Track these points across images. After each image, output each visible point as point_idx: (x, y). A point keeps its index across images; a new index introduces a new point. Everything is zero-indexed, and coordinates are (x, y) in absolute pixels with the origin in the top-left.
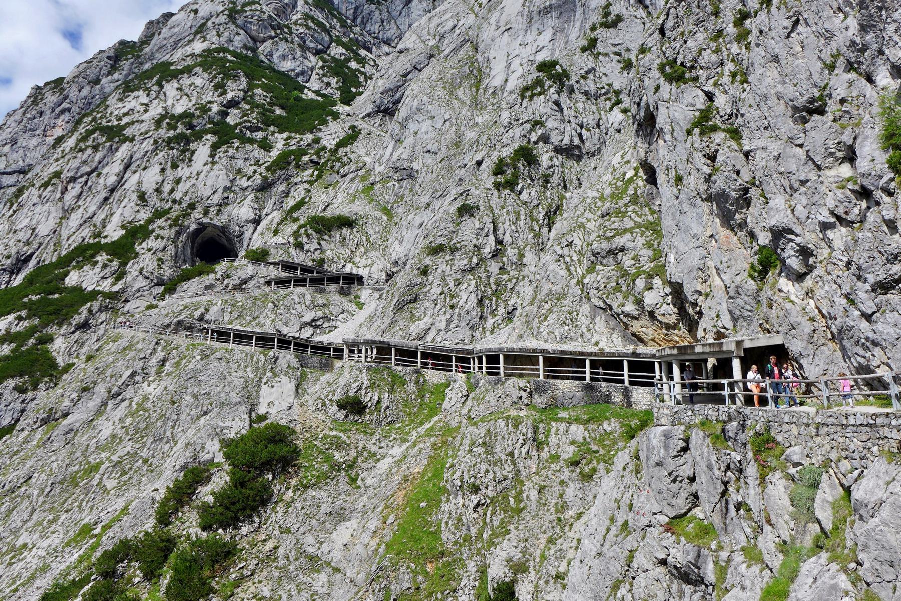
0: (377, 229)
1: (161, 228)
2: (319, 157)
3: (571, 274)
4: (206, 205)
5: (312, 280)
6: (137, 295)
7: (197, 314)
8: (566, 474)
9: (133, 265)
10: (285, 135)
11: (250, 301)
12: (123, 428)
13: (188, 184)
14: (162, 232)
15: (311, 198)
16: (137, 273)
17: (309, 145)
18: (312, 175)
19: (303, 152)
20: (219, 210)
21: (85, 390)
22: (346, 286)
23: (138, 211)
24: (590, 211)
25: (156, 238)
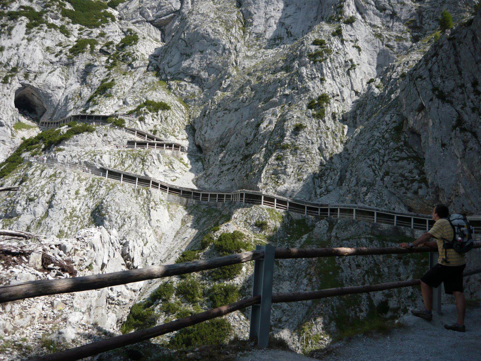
0: (181, 115)
2: (108, 48)
3: (376, 175)
5: (158, 145)
8: (397, 262)
10: (78, 26)
11: (124, 154)
12: (65, 226)
17: (97, 37)
18: (107, 61)
19: (93, 43)
20: (36, 76)
21: (31, 200)
22: (175, 151)
24: (379, 143)
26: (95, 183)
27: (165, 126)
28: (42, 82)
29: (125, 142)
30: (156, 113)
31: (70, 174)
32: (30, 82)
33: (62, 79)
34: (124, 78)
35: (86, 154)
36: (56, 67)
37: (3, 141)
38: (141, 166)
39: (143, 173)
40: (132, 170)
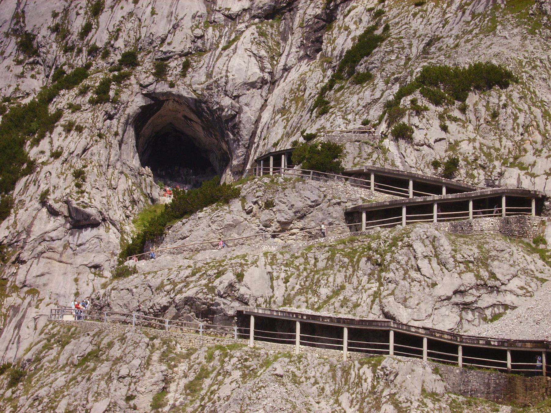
1: (75, 108)
4: (159, 55)
5: (444, 206)
6: (40, 248)
7: (221, 284)
9: (26, 187)
11: (322, 256)
13: (119, 14)
14: (77, 118)
15: (387, 28)
16: (37, 205)
20: (186, 66)
23: (22, 76)
25: (69, 128)
26: (216, 362)
27: (491, 140)
28: (203, 79)
29: (338, 212)
30: (458, 103)
31: (136, 344)
32: (172, 85)
33: (260, 59)
34: (415, 15)
35: (193, 274)
36: (241, 27)
37: (96, 267)
38: (375, 286)
39: (376, 307)
40: (344, 303)
